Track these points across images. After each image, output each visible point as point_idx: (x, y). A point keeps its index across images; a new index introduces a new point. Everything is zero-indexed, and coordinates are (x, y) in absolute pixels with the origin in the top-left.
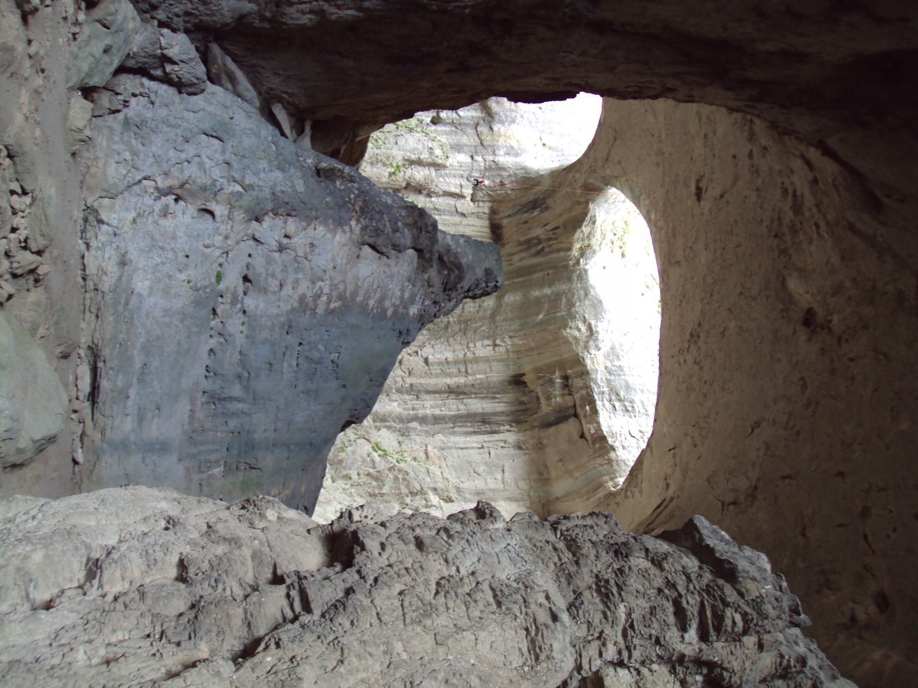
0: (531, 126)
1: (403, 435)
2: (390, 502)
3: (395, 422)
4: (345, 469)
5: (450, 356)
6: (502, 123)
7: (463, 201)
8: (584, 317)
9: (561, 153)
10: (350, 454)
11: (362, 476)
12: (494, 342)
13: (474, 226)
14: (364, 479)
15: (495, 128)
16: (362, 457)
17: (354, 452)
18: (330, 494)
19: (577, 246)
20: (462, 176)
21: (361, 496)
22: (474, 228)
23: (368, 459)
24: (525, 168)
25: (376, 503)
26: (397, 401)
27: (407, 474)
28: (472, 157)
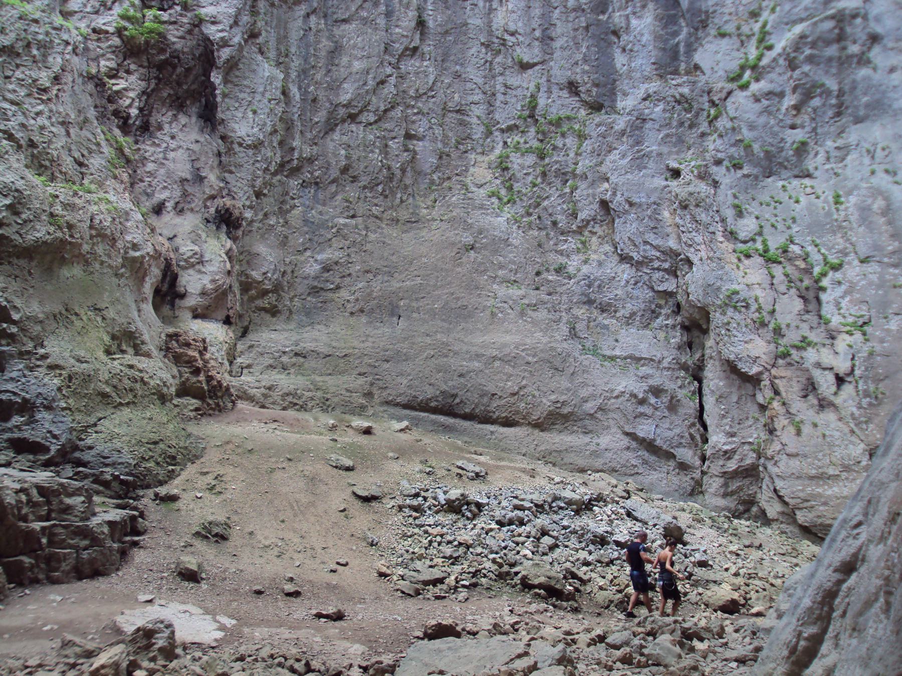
1: (704, 25)
2: (854, 81)
3: (676, 34)
4: (781, 150)
10: (754, 134)
11: (798, 121)
14: (804, 118)
16: (761, 113)
17: (752, 127)
18: (856, 187)
21: (842, 132)
23: (765, 103)
25: (856, 107)
26: (627, 17)
27: (803, 37)
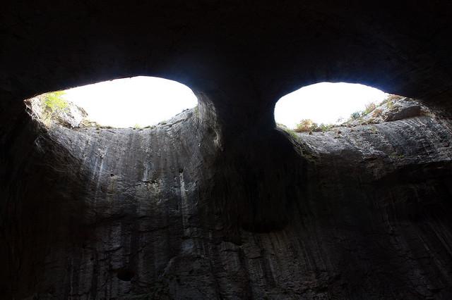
0: (134, 186)
5: (418, 272)
6: (134, 208)
7: (245, 252)
8: (361, 162)
9: (162, 171)
12: (391, 235)
13: (272, 244)
15: (143, 214)
19: (302, 155)
20: (215, 249)
22: (276, 244)
24: (199, 192)
28: (187, 238)
